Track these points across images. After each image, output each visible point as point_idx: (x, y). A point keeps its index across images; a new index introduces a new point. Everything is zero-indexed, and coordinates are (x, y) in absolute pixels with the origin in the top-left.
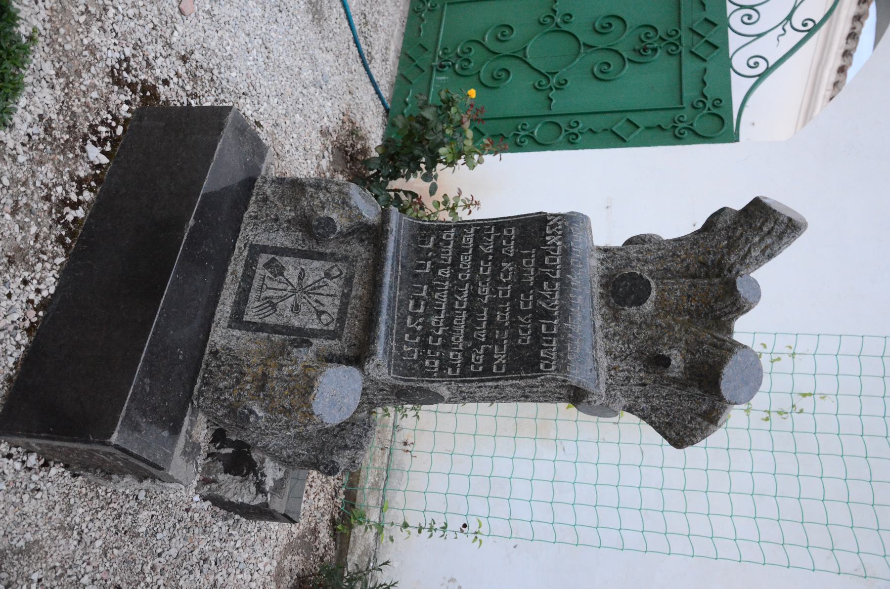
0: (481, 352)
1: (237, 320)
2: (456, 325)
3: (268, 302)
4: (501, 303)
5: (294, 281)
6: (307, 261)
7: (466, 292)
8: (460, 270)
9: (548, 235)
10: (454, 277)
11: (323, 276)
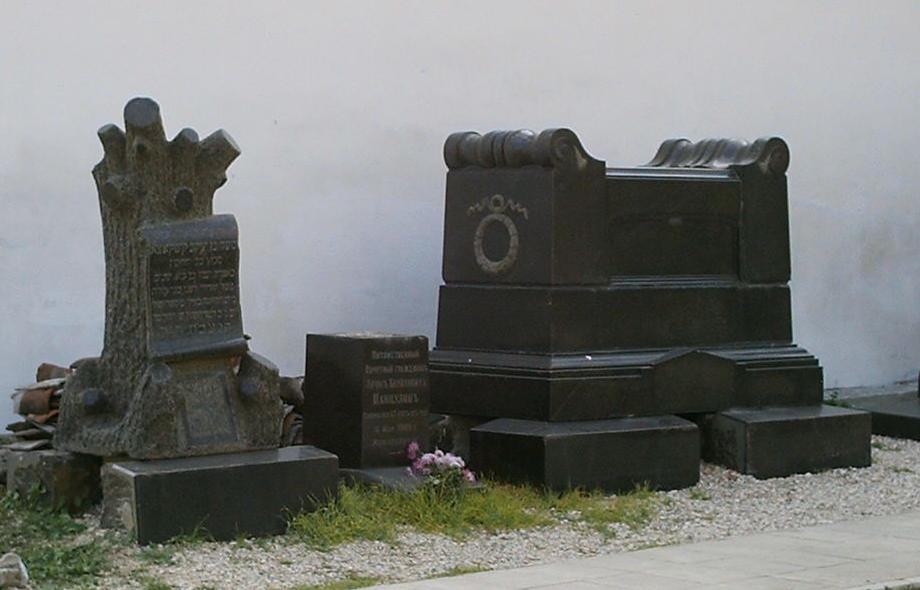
10: (183, 310)
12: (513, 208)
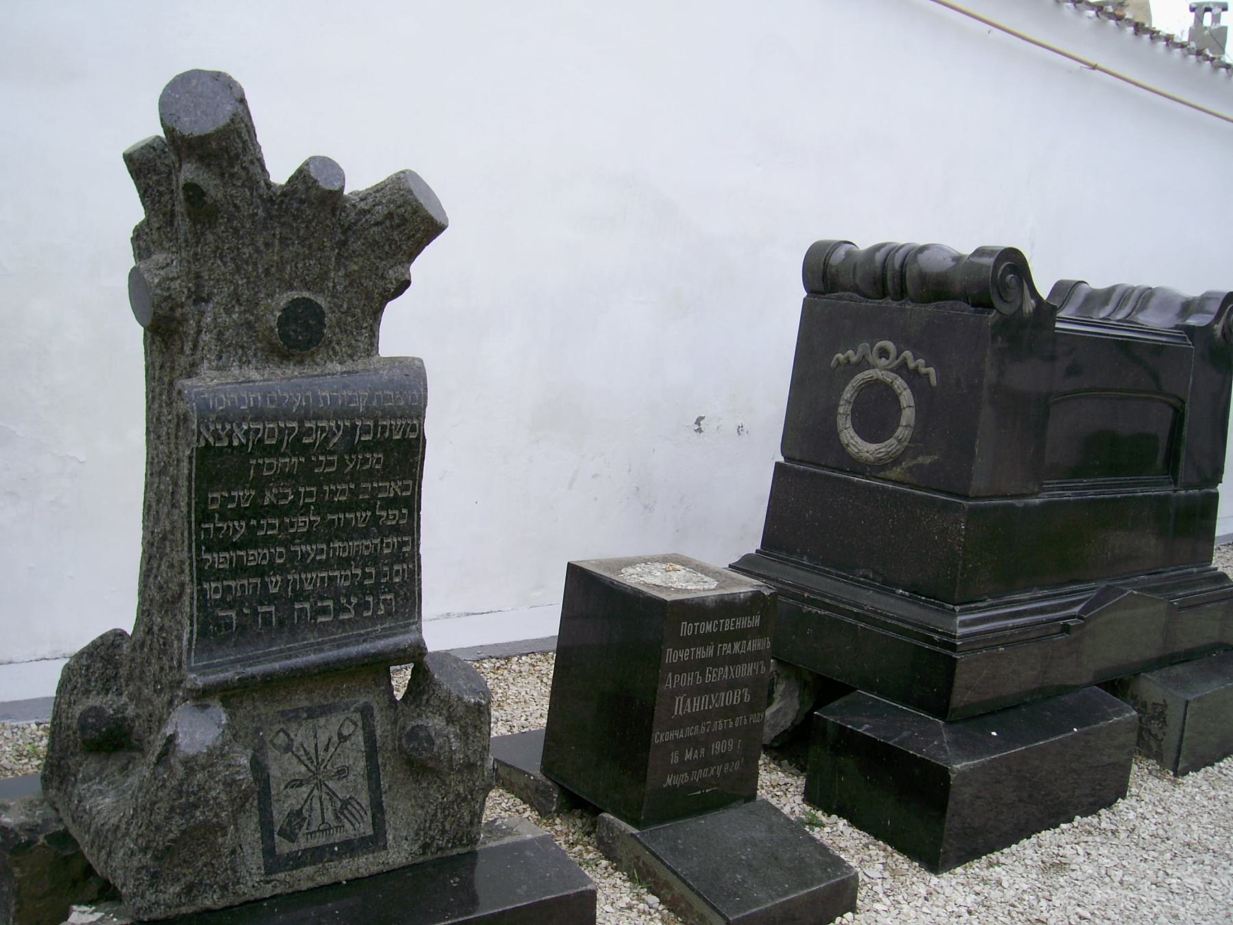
0: (384, 514)
1: (375, 841)
2: (349, 552)
3: (342, 813)
4: (324, 497)
5: (305, 790)
6: (273, 784)
7: (303, 548)
8: (272, 562)
9: (231, 442)
10: (282, 570)
11: (290, 753)
12: (911, 365)
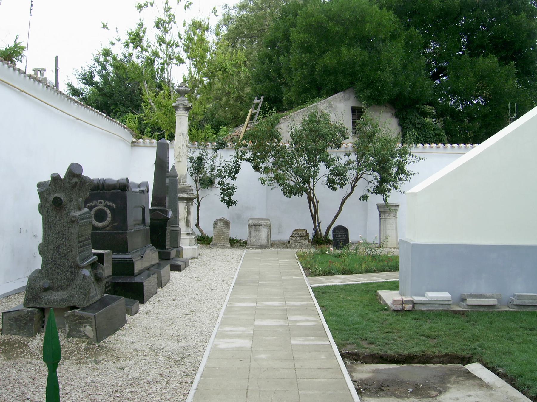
12: (108, 204)
